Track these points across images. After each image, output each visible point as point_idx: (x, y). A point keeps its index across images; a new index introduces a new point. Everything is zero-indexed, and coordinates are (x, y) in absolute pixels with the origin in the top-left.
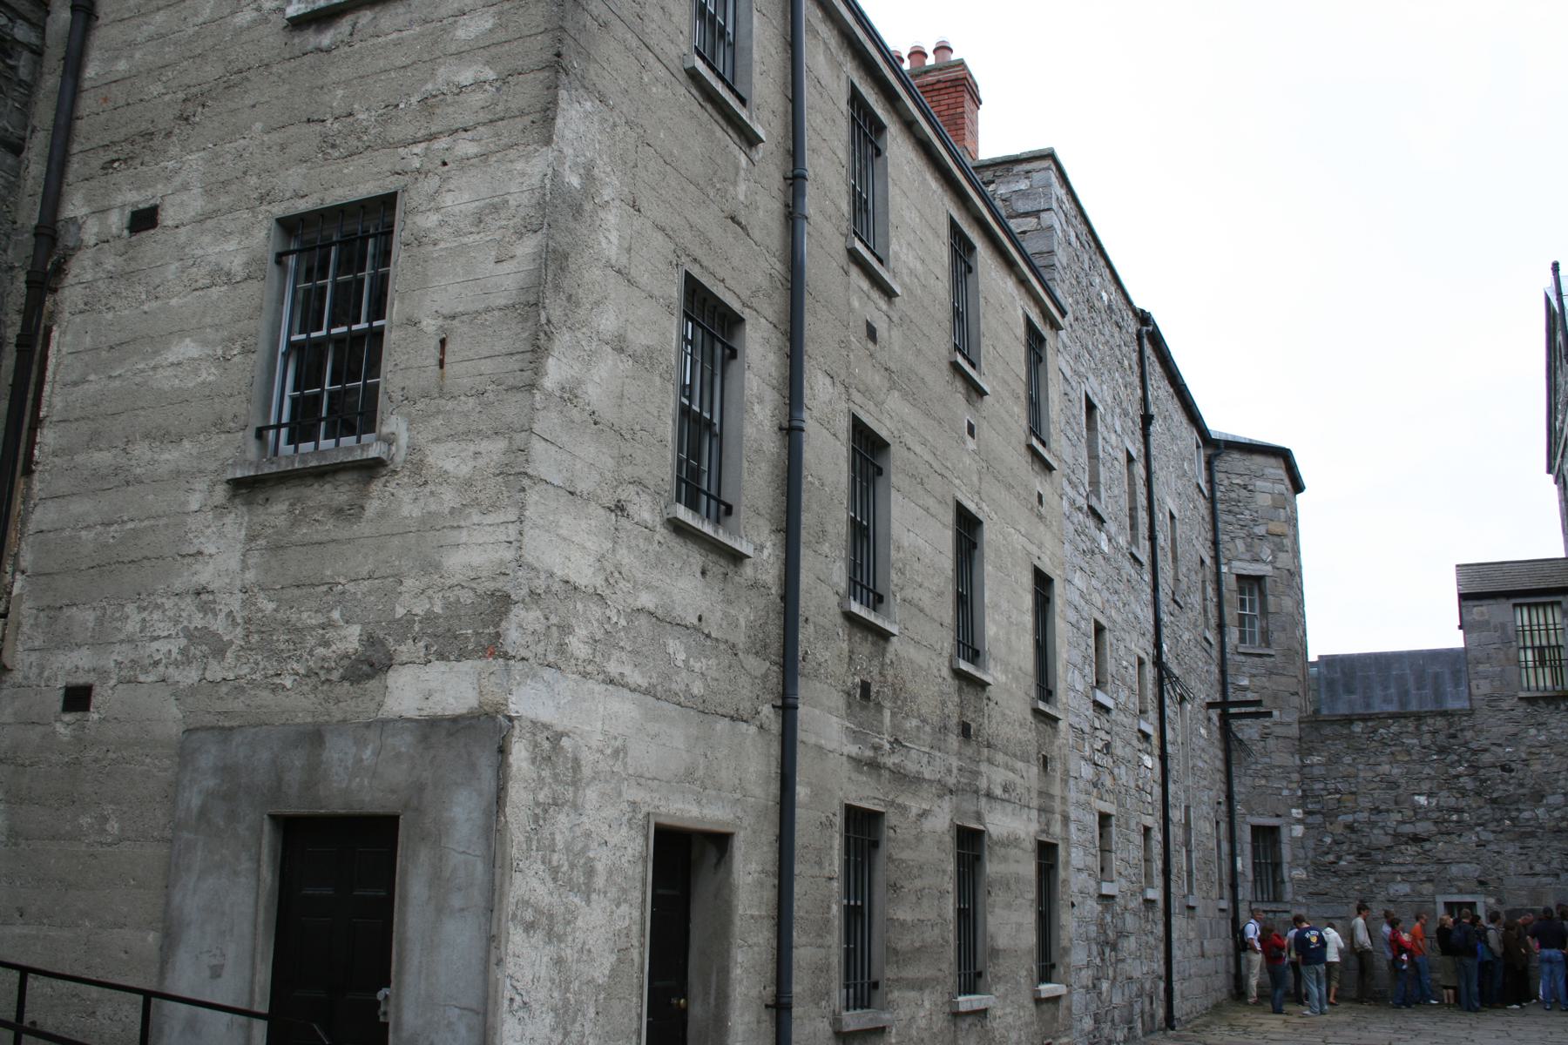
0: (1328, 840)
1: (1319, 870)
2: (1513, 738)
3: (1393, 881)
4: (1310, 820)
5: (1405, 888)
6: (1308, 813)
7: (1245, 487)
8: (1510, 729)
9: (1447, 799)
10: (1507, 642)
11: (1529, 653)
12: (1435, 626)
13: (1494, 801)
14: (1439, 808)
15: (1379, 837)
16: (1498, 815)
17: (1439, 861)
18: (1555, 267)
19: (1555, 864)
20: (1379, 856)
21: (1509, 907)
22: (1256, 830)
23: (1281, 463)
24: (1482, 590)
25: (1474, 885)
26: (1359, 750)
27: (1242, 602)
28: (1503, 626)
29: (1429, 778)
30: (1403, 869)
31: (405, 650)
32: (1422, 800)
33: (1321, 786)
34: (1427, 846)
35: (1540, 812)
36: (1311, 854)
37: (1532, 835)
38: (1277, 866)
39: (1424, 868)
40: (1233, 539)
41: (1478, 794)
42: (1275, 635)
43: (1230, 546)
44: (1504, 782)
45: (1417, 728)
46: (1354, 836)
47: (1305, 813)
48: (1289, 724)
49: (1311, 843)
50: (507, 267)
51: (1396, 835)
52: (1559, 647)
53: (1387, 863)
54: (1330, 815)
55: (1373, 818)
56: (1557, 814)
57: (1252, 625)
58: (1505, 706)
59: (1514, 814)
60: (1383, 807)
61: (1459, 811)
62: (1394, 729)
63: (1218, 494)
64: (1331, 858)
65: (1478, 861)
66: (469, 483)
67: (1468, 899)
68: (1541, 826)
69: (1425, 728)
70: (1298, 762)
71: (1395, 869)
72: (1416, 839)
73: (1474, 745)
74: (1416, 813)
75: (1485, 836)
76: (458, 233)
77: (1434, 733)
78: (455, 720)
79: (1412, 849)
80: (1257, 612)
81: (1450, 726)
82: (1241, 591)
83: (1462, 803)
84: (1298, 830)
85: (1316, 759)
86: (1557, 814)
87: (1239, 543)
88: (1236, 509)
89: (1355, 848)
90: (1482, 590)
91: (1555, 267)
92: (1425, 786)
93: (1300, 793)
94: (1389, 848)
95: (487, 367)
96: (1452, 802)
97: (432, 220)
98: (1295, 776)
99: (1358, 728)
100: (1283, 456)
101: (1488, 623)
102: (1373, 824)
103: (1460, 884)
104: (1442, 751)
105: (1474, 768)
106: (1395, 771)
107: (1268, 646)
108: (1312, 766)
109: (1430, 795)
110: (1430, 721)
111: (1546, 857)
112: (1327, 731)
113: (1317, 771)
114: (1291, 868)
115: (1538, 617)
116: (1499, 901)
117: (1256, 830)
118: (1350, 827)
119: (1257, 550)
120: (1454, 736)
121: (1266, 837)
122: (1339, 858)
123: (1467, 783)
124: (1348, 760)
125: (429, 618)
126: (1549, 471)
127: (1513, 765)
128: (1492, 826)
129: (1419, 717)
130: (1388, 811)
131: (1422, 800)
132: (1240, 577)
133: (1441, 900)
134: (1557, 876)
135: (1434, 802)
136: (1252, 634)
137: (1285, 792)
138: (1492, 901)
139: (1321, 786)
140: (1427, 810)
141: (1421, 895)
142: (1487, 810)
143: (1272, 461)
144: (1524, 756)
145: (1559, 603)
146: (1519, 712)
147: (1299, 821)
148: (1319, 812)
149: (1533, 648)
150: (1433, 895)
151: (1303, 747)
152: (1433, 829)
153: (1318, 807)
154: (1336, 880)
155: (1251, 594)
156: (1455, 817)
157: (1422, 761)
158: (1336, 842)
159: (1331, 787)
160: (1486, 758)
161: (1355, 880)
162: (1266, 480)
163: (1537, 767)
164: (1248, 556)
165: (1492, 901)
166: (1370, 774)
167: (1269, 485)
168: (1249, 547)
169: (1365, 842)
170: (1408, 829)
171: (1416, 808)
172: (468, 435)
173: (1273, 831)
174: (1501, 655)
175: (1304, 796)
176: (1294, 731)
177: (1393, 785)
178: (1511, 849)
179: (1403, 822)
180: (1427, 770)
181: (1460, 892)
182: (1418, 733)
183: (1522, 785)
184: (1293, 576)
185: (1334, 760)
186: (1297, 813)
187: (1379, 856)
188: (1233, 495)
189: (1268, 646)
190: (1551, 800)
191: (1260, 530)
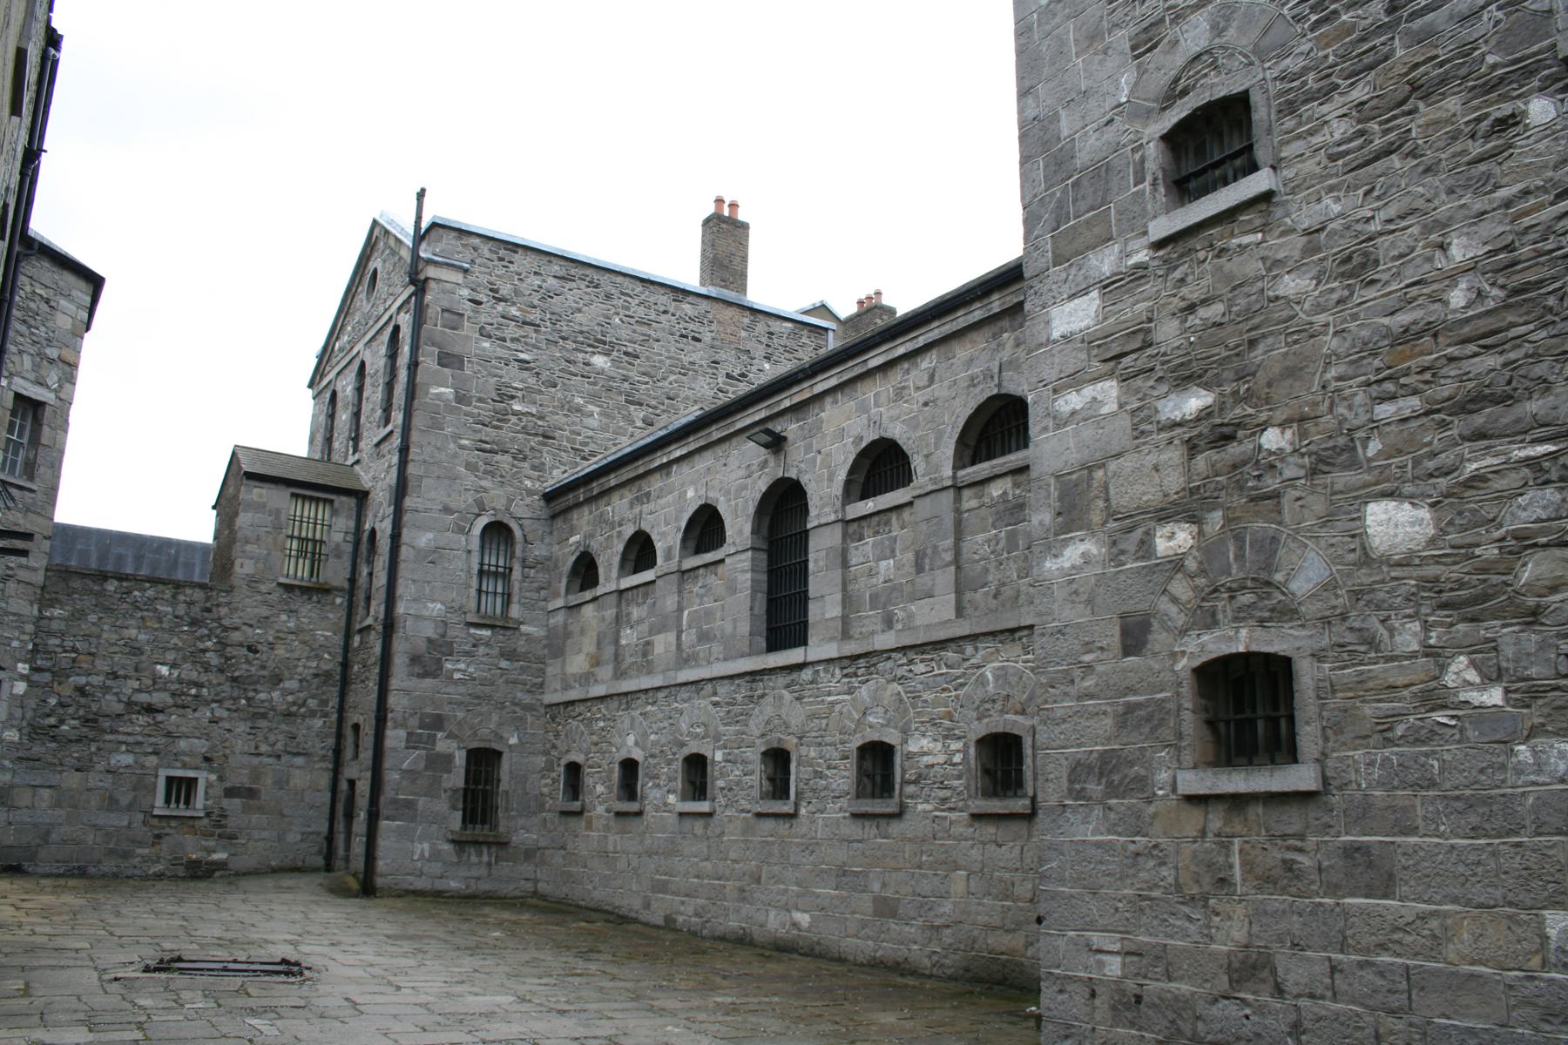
0: (53, 701)
2: (264, 621)
3: (117, 751)
4: (36, 677)
5: (128, 759)
6: (36, 670)
7: (47, 301)
8: (264, 611)
9: (189, 672)
10: (278, 528)
11: (295, 543)
13: (234, 679)
14: (180, 681)
15: (111, 704)
16: (235, 694)
17: (169, 734)
18: (421, 195)
19: (279, 746)
20: (106, 724)
21: (229, 785)
23: (90, 289)
24: (247, 476)
25: (199, 761)
26: (108, 610)
27: (12, 425)
28: (278, 512)
29: (176, 648)
30: (131, 739)
32: (164, 670)
33: (57, 642)
34: (160, 717)
35: (276, 694)
36: (29, 714)
37: (264, 716)
39: (152, 740)
40: (20, 352)
41: (221, 671)
42: (42, 469)
43: (16, 359)
44: (248, 662)
45: (174, 596)
46: (83, 700)
47: (31, 669)
48: (35, 570)
49: (32, 703)
51: (130, 703)
52: (322, 542)
53: (113, 732)
54: (59, 674)
55: (108, 683)
56: (290, 698)
57: (16, 454)
58: (263, 588)
59: (251, 694)
60: (121, 673)
61: (199, 685)
62: (150, 593)
63: (17, 298)
64: (52, 721)
65: (208, 737)
67: (191, 774)
68: (273, 709)
69: (182, 598)
70: (36, 612)
71: (122, 738)
72: (150, 709)
73: (226, 622)
74: (155, 683)
75: (221, 713)
77: (190, 603)
79: (143, 719)
80: (25, 440)
81: (208, 599)
82: (14, 413)
83: (204, 678)
84: (20, 688)
85: (57, 612)
86: (290, 698)
87: (25, 356)
88: (32, 322)
89: (81, 712)
90: (247, 476)
91: (421, 195)
92: (170, 656)
93: (30, 647)
94: (119, 716)
96: (194, 675)
98: (30, 628)
99: (111, 586)
100: (95, 282)
101: (264, 506)
102: (106, 689)
103: (186, 759)
104: (194, 623)
105: (223, 644)
106: (142, 637)
107: (31, 478)
108: (50, 619)
109: (173, 666)
110: (188, 591)
111: (272, 738)
112: (77, 584)
113: (55, 625)
115: (309, 510)
116: (221, 779)
118: (81, 690)
119: (44, 372)
120: (209, 610)
122: (62, 722)
123: (213, 659)
124: (93, 618)
126: (311, 386)
127: (259, 647)
128: (228, 704)
129: (178, 586)
130: (126, 677)
131: (164, 670)
132: (18, 396)
133: (163, 774)
134: (279, 757)
135: (176, 673)
136: (14, 463)
137: (15, 644)
138: (213, 777)
139: (57, 642)
140: (168, 681)
141: (143, 767)
142: (226, 687)
143: (82, 284)
144: (271, 639)
145: (332, 502)
146: (275, 597)
147: (23, 677)
149: (299, 538)
150: (156, 768)
151: (45, 597)
152: (170, 700)
153: (49, 664)
154: (54, 745)
155: (23, 419)
156: (193, 691)
157: (171, 631)
158: (61, 705)
159: (68, 644)
160: (236, 636)
161: (74, 747)
162: (73, 301)
163: (281, 651)
164: (32, 376)
165: (213, 777)
166: (115, 637)
167: (72, 307)
168: (36, 367)
169: (94, 707)
170: (143, 698)
171: (156, 678)
174: (270, 539)
175: (35, 650)
176: (39, 578)
177: (136, 650)
178: (242, 727)
179: (139, 691)
180: (175, 640)
181: (185, 766)
182: (173, 601)
183: (263, 667)
185: (78, 615)
186: (23, 668)
187: (106, 724)
188: (32, 305)
189: (31, 478)
190: (287, 684)
191: (52, 353)
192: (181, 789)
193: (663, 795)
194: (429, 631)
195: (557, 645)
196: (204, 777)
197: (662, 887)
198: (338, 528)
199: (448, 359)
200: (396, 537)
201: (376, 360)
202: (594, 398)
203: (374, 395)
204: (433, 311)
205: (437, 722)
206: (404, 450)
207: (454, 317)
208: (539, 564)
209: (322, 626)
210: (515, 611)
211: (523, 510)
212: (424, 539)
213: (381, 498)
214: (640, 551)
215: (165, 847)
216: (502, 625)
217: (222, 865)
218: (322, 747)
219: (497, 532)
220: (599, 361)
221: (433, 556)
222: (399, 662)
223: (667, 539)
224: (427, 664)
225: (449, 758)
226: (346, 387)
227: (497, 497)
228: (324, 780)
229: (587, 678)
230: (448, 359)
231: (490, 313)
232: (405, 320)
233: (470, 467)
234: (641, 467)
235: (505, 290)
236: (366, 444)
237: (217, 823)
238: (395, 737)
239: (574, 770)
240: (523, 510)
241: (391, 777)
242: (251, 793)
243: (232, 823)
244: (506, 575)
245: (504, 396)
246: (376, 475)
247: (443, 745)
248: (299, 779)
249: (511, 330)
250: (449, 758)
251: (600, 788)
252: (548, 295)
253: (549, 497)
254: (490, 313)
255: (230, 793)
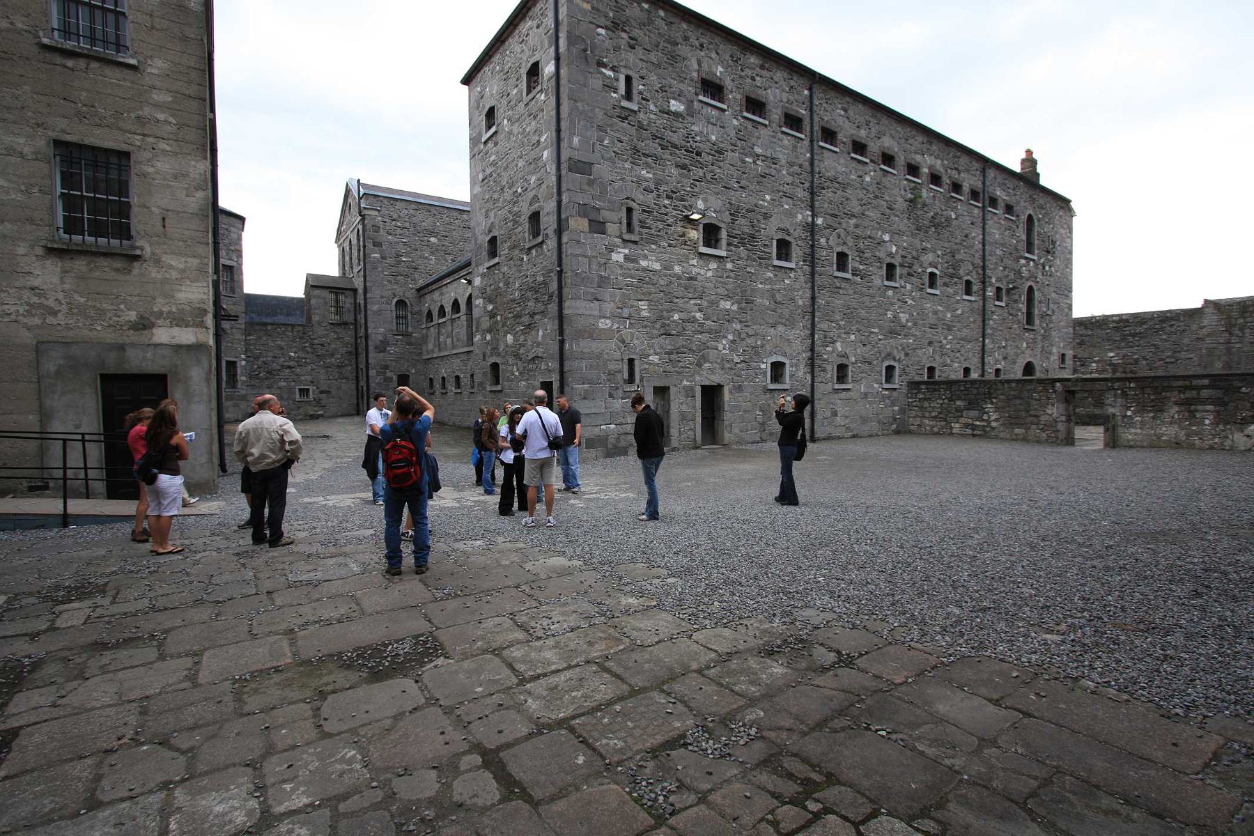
1: (251, 377)
9: (301, 354)
12: (296, 290)
22: (227, 362)
31: (160, 322)
38: (235, 375)
50: (192, 199)
66: (184, 271)
72: (289, 367)
76: (165, 179)
78: (189, 346)
84: (244, 363)
95: (187, 232)
97: (151, 170)
100: (242, 219)
114: (242, 374)
117: (227, 362)
121: (232, 365)
125: (170, 312)
148: (252, 358)
151: (247, 332)
171: (290, 357)
172: (180, 254)
173: (234, 363)
177: (281, 348)
178: (322, 371)
184: (240, 265)
185: (260, 338)
191: (232, 248)
192: (304, 392)
193: (451, 388)
194: (380, 338)
195: (425, 339)
196: (311, 388)
197: (452, 415)
198: (346, 301)
199: (377, 244)
200: (365, 307)
201: (354, 242)
202: (432, 253)
203: (355, 254)
204: (369, 226)
205: (386, 367)
206: (365, 277)
207: (376, 228)
208: (419, 313)
209: (348, 337)
210: (410, 329)
211: (410, 295)
212: (375, 308)
213: (361, 291)
214: (442, 312)
215: (301, 411)
216: (406, 334)
217: (322, 415)
218: (352, 376)
219: (401, 304)
220: (433, 239)
221: (379, 312)
222: (371, 349)
223: (448, 309)
224: (382, 348)
225: (391, 379)
226: (346, 245)
227: (400, 292)
228: (354, 387)
229: (433, 351)
230: (377, 244)
231: (390, 225)
232: (360, 227)
233: (389, 282)
234: (440, 284)
235: (395, 216)
236: (355, 270)
237: (318, 402)
238: (372, 373)
239: (431, 380)
240: (410, 295)
241: (372, 385)
242: (329, 392)
243: (323, 402)
244: (406, 317)
245: (399, 255)
246: (358, 283)
247: (389, 374)
248: (344, 387)
249: (399, 231)
250: (391, 379)
251: (437, 385)
252: (411, 216)
253: (418, 290)
254: (390, 225)
255: (322, 392)
